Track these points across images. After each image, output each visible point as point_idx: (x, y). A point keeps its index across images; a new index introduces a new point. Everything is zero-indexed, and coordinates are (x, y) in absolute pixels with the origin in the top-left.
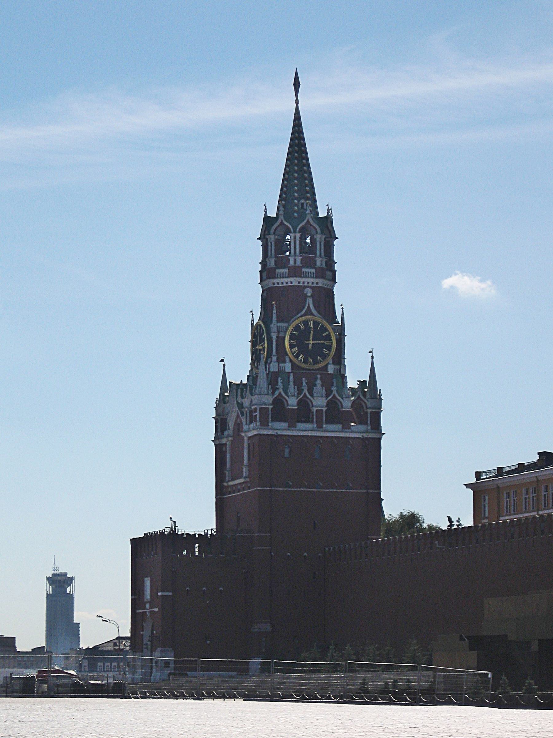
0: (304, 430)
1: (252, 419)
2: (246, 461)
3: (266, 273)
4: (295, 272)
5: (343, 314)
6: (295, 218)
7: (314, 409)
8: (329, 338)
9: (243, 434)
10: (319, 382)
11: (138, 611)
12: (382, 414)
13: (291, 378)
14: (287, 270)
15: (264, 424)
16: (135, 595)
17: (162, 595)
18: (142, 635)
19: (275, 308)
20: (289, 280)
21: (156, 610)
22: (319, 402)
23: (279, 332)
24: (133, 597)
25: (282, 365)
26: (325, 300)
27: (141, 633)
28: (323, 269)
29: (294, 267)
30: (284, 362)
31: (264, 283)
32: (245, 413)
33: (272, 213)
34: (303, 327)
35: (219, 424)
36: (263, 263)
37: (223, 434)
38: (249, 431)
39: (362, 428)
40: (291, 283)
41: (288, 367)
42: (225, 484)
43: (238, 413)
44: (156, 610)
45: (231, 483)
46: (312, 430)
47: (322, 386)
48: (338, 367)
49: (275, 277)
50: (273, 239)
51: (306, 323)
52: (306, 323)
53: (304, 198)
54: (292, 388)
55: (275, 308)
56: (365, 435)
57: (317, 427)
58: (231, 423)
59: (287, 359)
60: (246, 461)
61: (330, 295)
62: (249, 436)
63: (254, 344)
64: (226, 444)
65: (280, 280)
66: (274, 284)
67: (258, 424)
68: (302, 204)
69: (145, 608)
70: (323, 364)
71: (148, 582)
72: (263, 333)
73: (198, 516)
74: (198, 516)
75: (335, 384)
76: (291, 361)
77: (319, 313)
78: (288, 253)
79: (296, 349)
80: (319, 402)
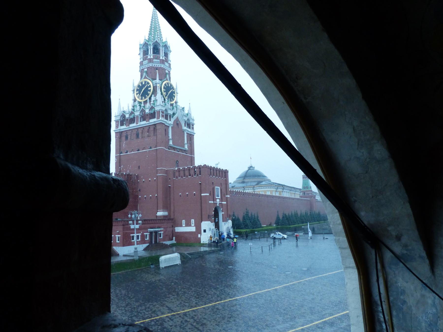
4: (162, 62)
8: (174, 93)
12: (194, 126)
14: (159, 61)
20: (160, 65)
29: (163, 60)
39: (189, 130)
49: (153, 62)
50: (152, 47)
51: (168, 83)
65: (156, 65)
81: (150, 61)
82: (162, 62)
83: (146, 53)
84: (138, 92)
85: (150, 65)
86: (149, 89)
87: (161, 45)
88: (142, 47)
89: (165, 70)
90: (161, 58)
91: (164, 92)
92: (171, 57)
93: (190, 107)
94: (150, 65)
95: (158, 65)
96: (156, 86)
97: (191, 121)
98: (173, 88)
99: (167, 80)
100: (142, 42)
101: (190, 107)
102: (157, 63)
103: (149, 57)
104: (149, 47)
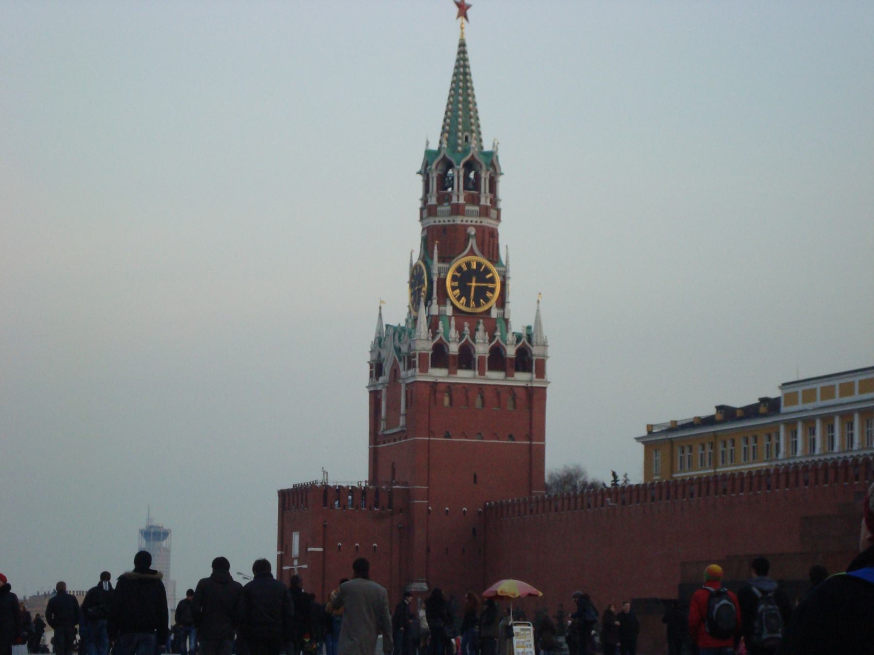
0: (464, 376)
1: (411, 365)
2: (403, 409)
3: (427, 210)
4: (457, 210)
5: (507, 257)
6: (459, 152)
7: (477, 357)
9: (400, 381)
10: (481, 327)
11: (285, 568)
13: (453, 322)
14: (449, 208)
15: (424, 370)
17: (312, 552)
20: (451, 219)
21: (305, 566)
22: (482, 349)
23: (439, 274)
24: (279, 553)
25: (442, 308)
26: (489, 242)
28: (487, 208)
30: (445, 304)
31: (426, 221)
33: (434, 146)
34: (465, 268)
35: (374, 370)
36: (425, 200)
37: (378, 380)
38: (408, 378)
41: (449, 310)
44: (305, 566)
45: (387, 432)
46: (475, 378)
47: (485, 331)
48: (501, 311)
52: (468, 264)
53: (468, 130)
54: (453, 333)
56: (530, 385)
57: (480, 374)
58: (387, 369)
59: (448, 303)
60: (403, 409)
61: (493, 234)
63: (412, 285)
65: (442, 219)
67: (418, 370)
68: (466, 138)
70: (486, 308)
71: (296, 538)
72: (423, 273)
73: (351, 468)
74: (351, 468)
75: (499, 329)
76: (452, 304)
77: (483, 253)
78: (450, 189)
79: (458, 291)
80: (482, 349)
82: (457, 210)
85: (431, 221)
88: (423, 171)
89: (465, 227)
90: (454, 200)
91: (453, 288)
93: (538, 311)
94: (431, 221)
95: (446, 219)
98: (487, 271)
99: (472, 252)
101: (538, 311)
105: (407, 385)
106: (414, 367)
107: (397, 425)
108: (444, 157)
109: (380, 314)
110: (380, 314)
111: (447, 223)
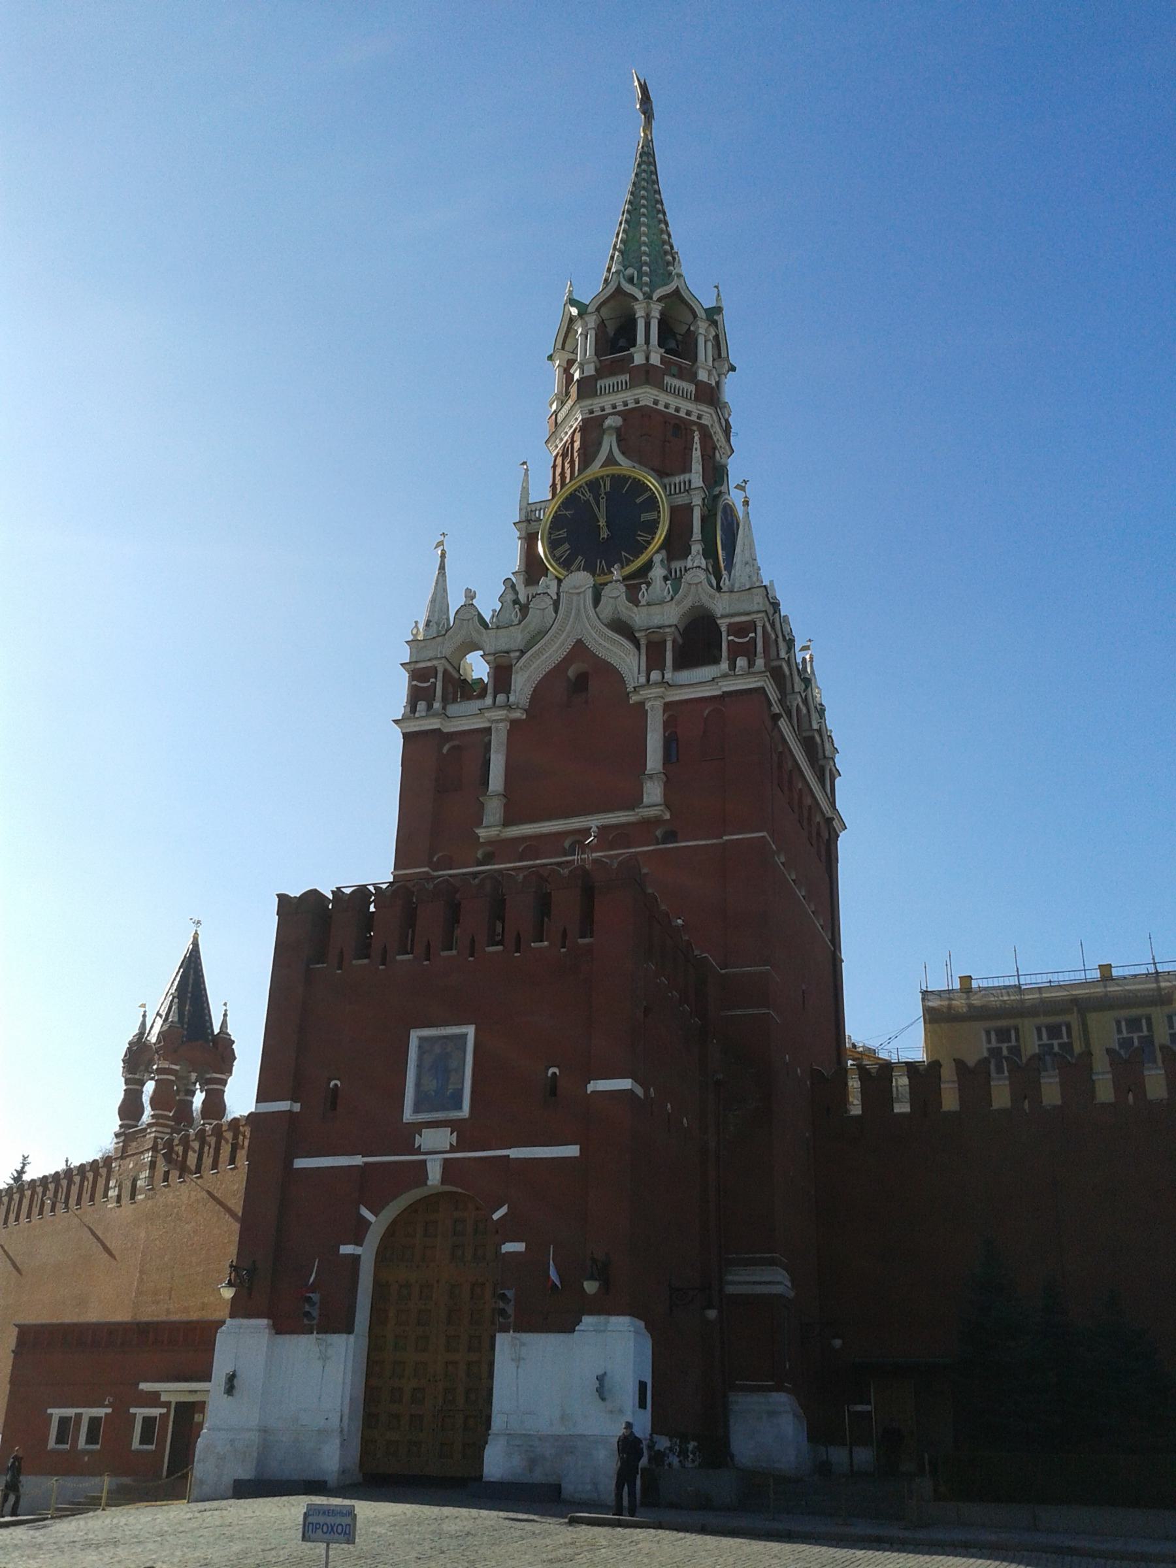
1: (685, 660)
11: (300, 1163)
12: (838, 781)
14: (692, 388)
16: (294, 1100)
18: (356, 1259)
19: (696, 439)
24: (283, 1106)
27: (346, 1249)
32: (643, 642)
37: (444, 708)
40: (699, 417)
42: (482, 833)
43: (580, 648)
50: (656, 314)
55: (696, 439)
62: (668, 699)
64: (488, 731)
65: (674, 402)
66: (656, 402)
67: (760, 662)
69: (418, 1151)
81: (648, 375)
83: (615, 335)
84: (563, 533)
85: (646, 396)
86: (644, 517)
87: (701, 314)
90: (703, 376)
92: (732, 390)
94: (646, 396)
95: (685, 406)
96: (689, 508)
97: (827, 746)
100: (591, 290)
102: (676, 392)
103: (639, 359)
104: (640, 313)
105: (668, 706)
106: (749, 651)
107: (634, 800)
108: (677, 292)
109: (442, 567)
110: (442, 567)
111: (682, 414)
